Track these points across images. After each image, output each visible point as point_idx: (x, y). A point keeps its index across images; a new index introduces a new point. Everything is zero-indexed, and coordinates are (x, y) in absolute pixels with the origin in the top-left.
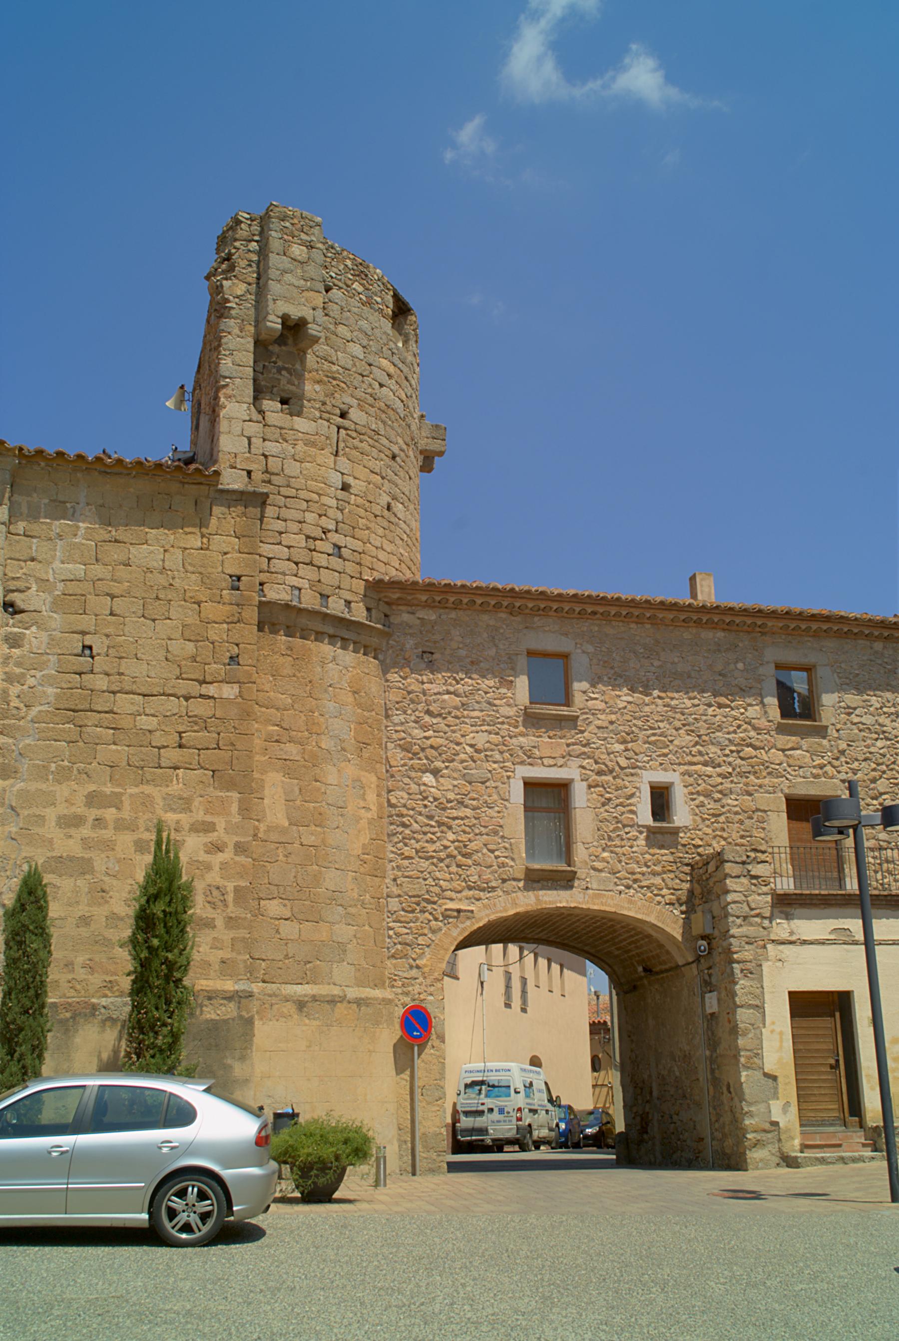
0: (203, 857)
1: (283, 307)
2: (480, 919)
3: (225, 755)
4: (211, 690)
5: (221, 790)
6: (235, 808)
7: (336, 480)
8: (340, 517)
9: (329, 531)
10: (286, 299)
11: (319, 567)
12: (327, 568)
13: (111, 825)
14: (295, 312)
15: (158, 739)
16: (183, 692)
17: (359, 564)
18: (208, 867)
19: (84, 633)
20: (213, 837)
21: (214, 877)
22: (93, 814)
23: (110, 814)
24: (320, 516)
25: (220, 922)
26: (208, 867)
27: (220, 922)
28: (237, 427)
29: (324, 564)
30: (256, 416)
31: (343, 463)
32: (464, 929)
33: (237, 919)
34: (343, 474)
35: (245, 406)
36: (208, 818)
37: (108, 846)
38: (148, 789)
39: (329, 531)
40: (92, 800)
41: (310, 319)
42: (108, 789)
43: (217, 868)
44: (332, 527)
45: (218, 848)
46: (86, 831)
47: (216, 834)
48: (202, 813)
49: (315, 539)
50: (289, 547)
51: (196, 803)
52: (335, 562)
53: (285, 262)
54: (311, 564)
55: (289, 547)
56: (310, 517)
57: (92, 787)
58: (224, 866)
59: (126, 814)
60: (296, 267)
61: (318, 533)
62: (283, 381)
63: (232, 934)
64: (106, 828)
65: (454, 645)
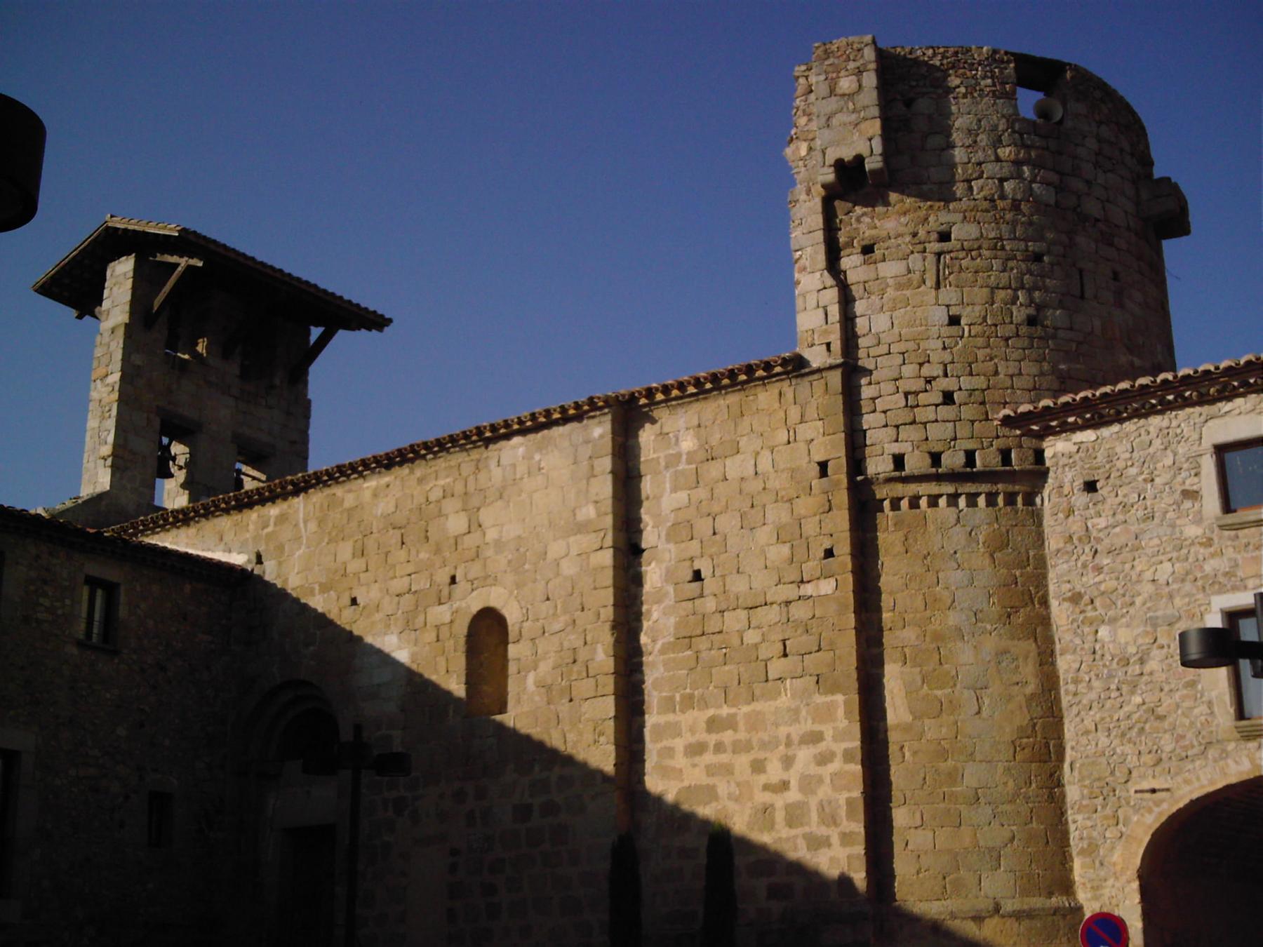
0: (814, 770)
1: (831, 157)
2: (1181, 798)
3: (825, 656)
4: (808, 589)
5: (826, 694)
6: (841, 712)
7: (940, 315)
8: (947, 357)
9: (935, 378)
10: (836, 143)
11: (925, 424)
12: (936, 421)
13: (729, 749)
14: (847, 154)
15: (764, 653)
16: (784, 598)
17: (983, 403)
18: (820, 780)
19: (692, 559)
20: (822, 746)
21: (824, 791)
22: (712, 739)
23: (728, 736)
24: (921, 365)
25: (835, 840)
26: (820, 780)
27: (835, 840)
28: (812, 300)
29: (932, 417)
30: (829, 281)
31: (949, 294)
32: (1160, 814)
33: (851, 833)
34: (948, 306)
35: (818, 275)
36: (817, 727)
37: (727, 770)
38: (757, 706)
39: (935, 378)
40: (713, 725)
41: (866, 152)
42: (725, 711)
43: (828, 780)
44: (938, 371)
45: (823, 759)
46: (709, 758)
47: (824, 743)
48: (810, 721)
49: (916, 393)
50: (885, 412)
51: (804, 713)
52: (946, 412)
53: (833, 103)
54: (913, 422)
55: (885, 412)
56: (908, 370)
57: (711, 712)
58: (834, 775)
59: (742, 735)
60: (846, 103)
61: (919, 384)
62: (863, 227)
63: (848, 850)
64: (725, 751)
65: (1120, 464)
